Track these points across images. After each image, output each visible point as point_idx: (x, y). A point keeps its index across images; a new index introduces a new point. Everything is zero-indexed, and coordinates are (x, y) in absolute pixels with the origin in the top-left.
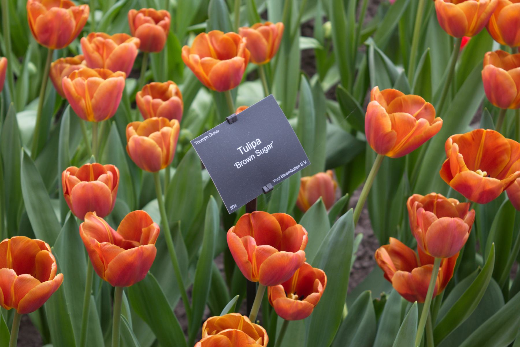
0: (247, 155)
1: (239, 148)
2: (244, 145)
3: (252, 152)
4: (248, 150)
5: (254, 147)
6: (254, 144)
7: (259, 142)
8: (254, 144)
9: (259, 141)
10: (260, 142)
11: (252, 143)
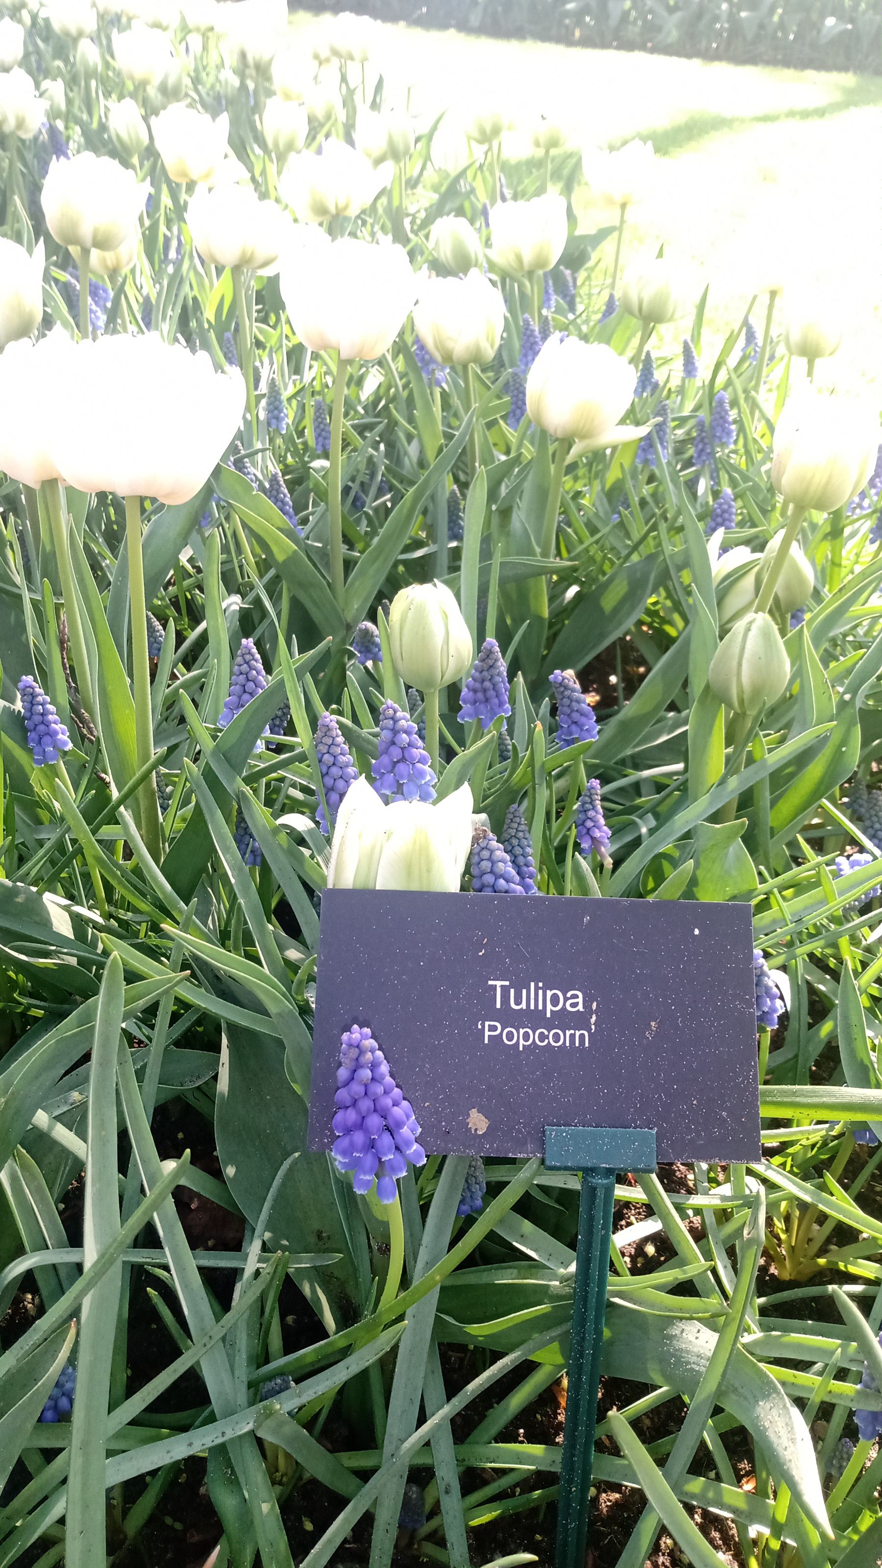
0: (509, 1018)
1: (499, 983)
2: (520, 985)
3: (534, 1019)
4: (524, 1006)
5: (549, 1007)
6: (555, 1001)
7: (575, 1001)
8: (555, 1001)
9: (580, 1000)
10: (580, 1008)
11: (549, 993)
